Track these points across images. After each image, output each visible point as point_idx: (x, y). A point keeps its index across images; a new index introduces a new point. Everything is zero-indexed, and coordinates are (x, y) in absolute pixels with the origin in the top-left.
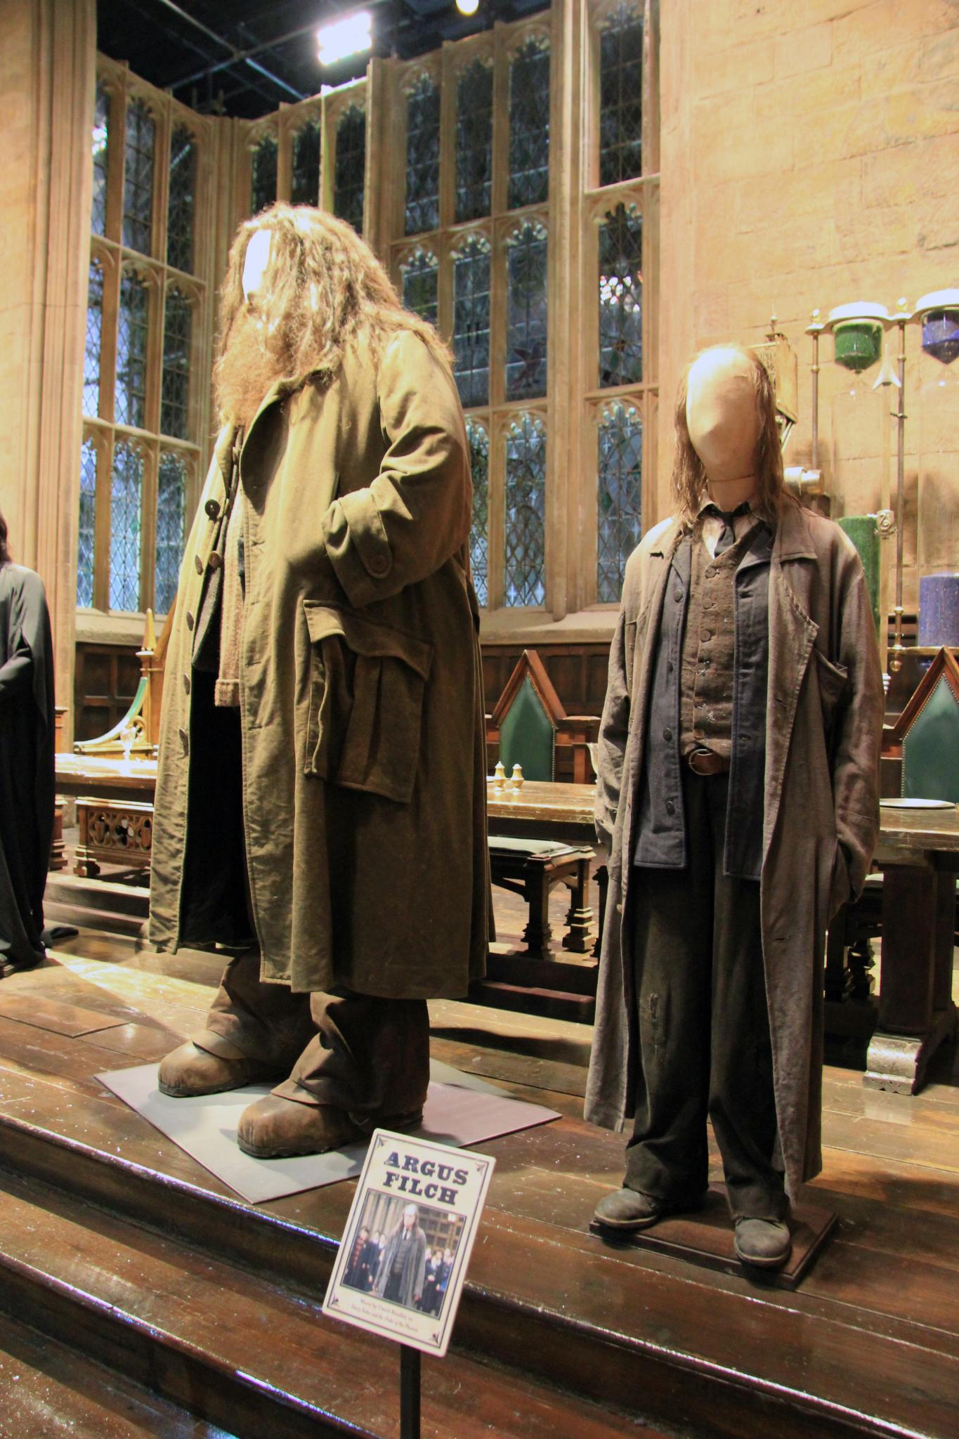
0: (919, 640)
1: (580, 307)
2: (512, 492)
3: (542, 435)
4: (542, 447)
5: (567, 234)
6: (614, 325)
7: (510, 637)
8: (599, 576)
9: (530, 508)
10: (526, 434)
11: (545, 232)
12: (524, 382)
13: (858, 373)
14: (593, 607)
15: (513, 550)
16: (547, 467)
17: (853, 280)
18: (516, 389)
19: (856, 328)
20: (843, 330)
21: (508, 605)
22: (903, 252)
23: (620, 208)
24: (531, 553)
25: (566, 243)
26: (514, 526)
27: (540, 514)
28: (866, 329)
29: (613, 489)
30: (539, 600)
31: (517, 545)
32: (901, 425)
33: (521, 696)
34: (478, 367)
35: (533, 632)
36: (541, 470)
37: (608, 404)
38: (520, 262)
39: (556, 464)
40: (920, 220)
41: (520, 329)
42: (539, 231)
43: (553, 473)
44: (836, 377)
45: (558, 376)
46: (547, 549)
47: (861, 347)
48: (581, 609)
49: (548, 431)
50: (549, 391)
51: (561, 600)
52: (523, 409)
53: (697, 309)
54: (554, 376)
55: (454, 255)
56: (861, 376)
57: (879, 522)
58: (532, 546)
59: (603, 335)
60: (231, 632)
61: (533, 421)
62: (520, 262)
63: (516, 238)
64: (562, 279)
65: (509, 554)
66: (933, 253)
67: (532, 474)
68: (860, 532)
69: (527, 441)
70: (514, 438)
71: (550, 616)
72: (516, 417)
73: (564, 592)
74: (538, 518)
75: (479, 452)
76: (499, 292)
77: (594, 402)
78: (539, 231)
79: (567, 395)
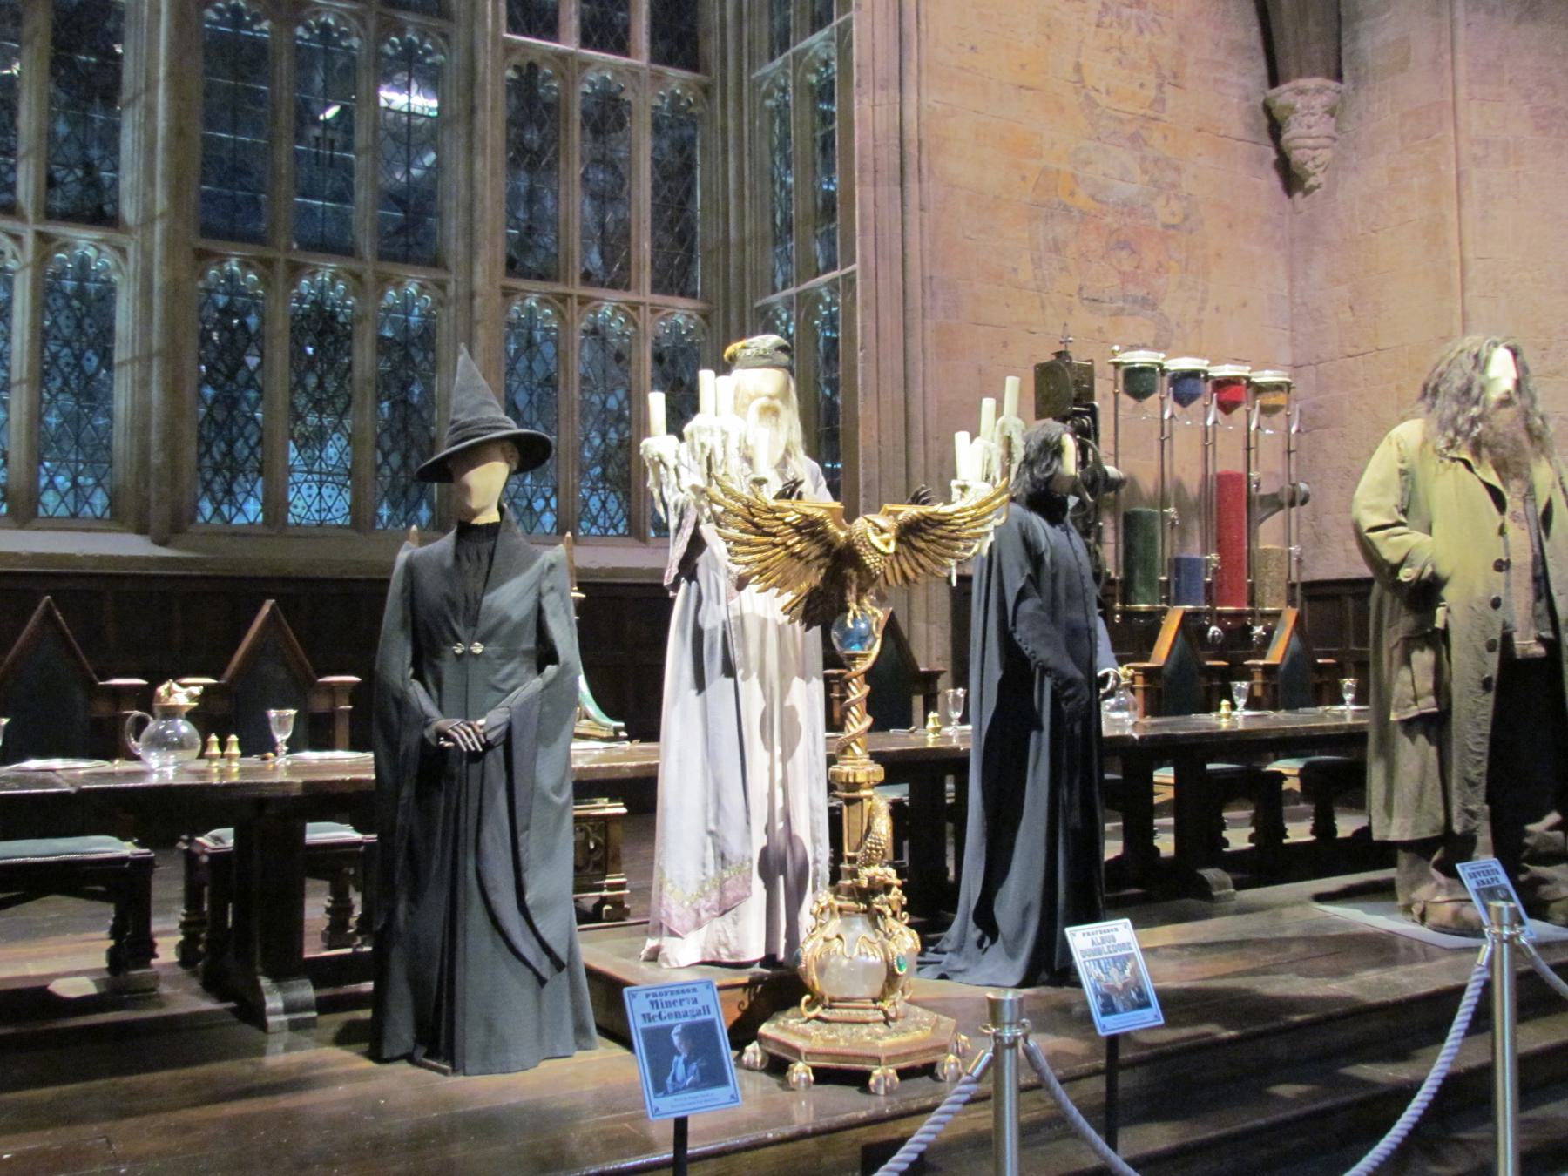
6: (522, 206)
12: (402, 239)
15: (386, 455)
23: (533, 67)
37: (524, 298)
55: (300, 31)
59: (511, 213)
65: (380, 460)
70: (388, 310)
77: (508, 293)
78: (428, 53)
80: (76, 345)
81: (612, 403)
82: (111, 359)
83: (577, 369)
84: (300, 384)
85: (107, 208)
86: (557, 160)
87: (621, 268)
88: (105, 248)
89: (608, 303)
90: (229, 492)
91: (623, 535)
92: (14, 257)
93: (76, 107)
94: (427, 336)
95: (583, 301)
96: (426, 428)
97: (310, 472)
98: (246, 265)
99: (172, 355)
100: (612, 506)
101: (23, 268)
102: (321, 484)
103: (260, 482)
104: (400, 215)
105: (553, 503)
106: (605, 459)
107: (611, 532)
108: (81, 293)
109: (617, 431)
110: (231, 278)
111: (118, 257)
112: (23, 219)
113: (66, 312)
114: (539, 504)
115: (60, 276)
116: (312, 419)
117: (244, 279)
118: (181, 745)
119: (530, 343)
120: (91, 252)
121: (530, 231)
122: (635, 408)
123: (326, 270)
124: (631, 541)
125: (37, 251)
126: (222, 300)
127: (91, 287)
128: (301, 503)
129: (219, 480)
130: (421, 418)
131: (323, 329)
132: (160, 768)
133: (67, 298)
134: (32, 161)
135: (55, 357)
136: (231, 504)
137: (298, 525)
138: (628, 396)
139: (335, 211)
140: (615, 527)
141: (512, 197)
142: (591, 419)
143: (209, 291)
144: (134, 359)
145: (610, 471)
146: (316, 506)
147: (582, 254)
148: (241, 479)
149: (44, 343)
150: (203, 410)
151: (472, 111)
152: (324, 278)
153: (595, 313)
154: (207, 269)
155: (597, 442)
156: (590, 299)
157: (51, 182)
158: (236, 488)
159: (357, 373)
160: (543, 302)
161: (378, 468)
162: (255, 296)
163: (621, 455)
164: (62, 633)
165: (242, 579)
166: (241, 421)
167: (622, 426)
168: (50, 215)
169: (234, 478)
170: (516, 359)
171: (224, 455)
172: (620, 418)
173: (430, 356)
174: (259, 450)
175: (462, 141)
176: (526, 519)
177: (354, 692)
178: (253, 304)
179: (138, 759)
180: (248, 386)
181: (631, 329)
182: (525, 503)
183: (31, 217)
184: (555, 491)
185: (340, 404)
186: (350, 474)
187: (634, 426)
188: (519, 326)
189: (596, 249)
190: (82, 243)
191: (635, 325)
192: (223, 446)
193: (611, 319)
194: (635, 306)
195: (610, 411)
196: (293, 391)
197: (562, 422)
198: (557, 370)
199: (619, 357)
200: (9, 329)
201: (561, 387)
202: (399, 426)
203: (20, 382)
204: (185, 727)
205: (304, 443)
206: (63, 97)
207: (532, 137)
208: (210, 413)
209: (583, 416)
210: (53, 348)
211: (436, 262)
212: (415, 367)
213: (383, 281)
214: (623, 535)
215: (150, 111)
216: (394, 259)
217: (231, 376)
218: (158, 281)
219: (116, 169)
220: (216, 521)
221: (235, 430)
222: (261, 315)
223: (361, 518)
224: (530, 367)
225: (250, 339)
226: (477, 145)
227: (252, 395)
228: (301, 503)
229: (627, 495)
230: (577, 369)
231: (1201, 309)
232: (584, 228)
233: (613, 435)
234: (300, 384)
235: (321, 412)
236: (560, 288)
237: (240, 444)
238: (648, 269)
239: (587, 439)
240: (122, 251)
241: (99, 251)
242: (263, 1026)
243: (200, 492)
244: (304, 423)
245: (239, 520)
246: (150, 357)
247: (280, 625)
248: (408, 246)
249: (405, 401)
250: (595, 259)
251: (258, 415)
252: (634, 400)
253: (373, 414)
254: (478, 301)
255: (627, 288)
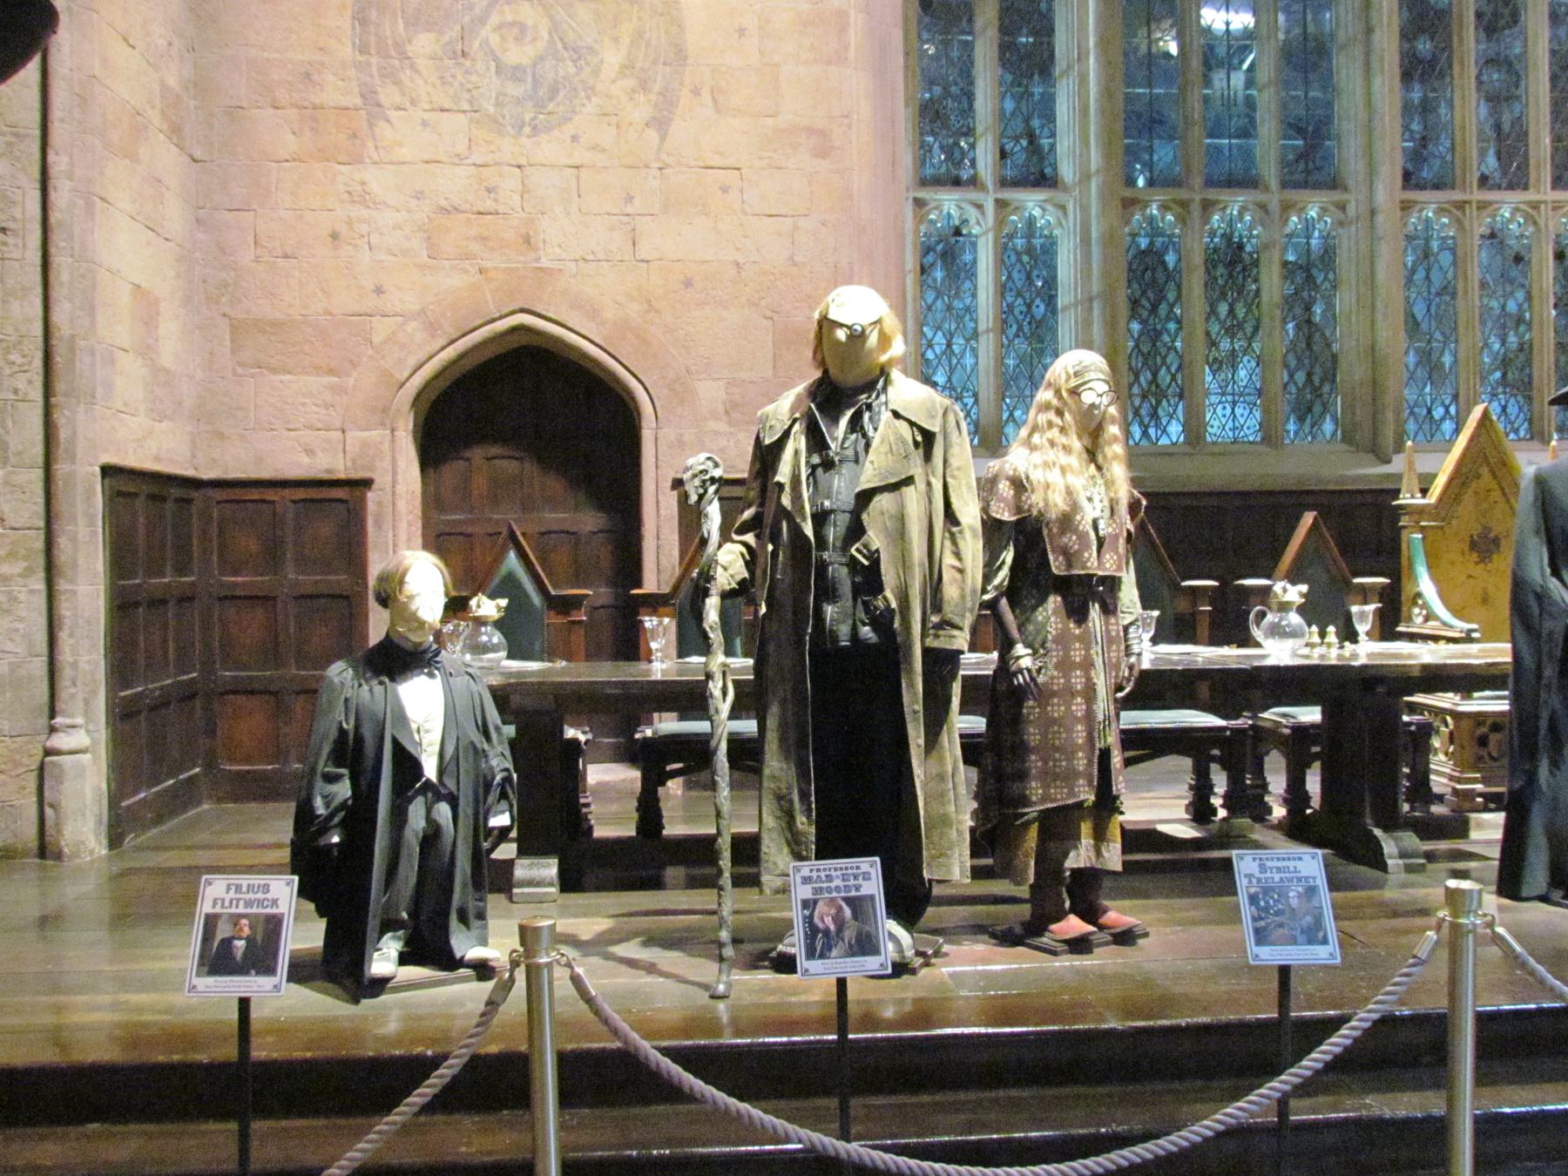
2: (1288, 303)
7: (1336, 483)
12: (1302, 166)
18: (1291, 173)
21: (1287, 441)
29: (1419, 311)
34: (1238, 137)
37: (1421, 210)
59: (1406, 128)
60: (402, 464)
65: (1286, 378)
70: (1290, 236)
75: (1241, 247)
77: (1406, 207)
80: (1027, 295)
81: (1512, 306)
82: (1055, 305)
83: (1475, 274)
84: (1213, 312)
85: (1048, 171)
86: (1450, 67)
87: (1518, 168)
88: (1049, 207)
89: (1507, 207)
90: (1154, 415)
91: (1524, 439)
92: (978, 223)
93: (1020, 85)
94: (1328, 255)
95: (1482, 206)
96: (1328, 346)
97: (1223, 394)
98: (1164, 207)
99: (1108, 296)
100: (1512, 410)
101: (985, 233)
102: (1234, 403)
103: (1180, 406)
104: (1301, 142)
105: (1452, 410)
106: (1505, 363)
107: (1512, 436)
108: (1030, 250)
109: (1517, 334)
110: (1151, 220)
111: (1060, 214)
112: (983, 188)
113: (1018, 266)
114: (1438, 413)
115: (1011, 237)
116: (1225, 345)
117: (1163, 220)
118: (1294, 634)
119: (1427, 254)
120: (1037, 212)
121: (1424, 141)
122: (1536, 309)
123: (1235, 202)
124: (1535, 444)
125: (996, 218)
126: (1143, 243)
127: (1037, 242)
128: (1216, 423)
129: (1146, 405)
130: (1323, 334)
131: (1232, 264)
132: (1277, 652)
133: (1018, 254)
134: (990, 138)
135: (1011, 306)
136: (1157, 426)
137: (1214, 443)
138: (1529, 297)
139: (1240, 147)
140: (1516, 431)
141: (1407, 109)
142: (1489, 324)
143: (1134, 235)
144: (1075, 305)
145: (1510, 375)
146: (1230, 424)
147: (1480, 159)
148: (1164, 403)
149: (1003, 296)
150: (1131, 344)
151: (1369, 31)
152: (1235, 212)
153: (1493, 216)
154: (1132, 215)
155: (1497, 346)
156: (1490, 203)
157: (1003, 154)
158: (1161, 412)
159: (1265, 297)
160: (1440, 211)
161: (1285, 386)
162: (1173, 235)
163: (1522, 357)
164: (1153, 543)
165: (1270, 493)
166: (1163, 351)
167: (1522, 328)
168: (1004, 183)
169: (1159, 403)
170: (1413, 271)
171: (1150, 383)
172: (1520, 320)
173: (1331, 276)
174: (1179, 377)
175: (1359, 64)
176: (1426, 427)
177: (1214, 596)
178: (1171, 242)
179: (1258, 645)
180: (1168, 319)
181: (1531, 229)
182: (1425, 411)
183: (991, 187)
184: (1455, 397)
185: (1249, 330)
186: (1260, 393)
187: (1535, 326)
188: (1417, 238)
189: (1492, 152)
190: (1030, 204)
191: (1535, 223)
192: (1149, 375)
193: (1510, 221)
194: (1535, 206)
195: (1510, 315)
196: (1207, 319)
197: (1461, 329)
198: (1455, 277)
199: (1518, 259)
200: (976, 287)
201: (1460, 294)
202: (1304, 345)
203: (988, 331)
204: (1294, 619)
205: (1216, 365)
206: (1009, 78)
207: (1424, 46)
208: (1137, 346)
209: (1483, 322)
210: (1010, 299)
211: (1334, 184)
212: (1316, 288)
213: (1287, 208)
214: (1524, 439)
215: (1083, 80)
216: (1297, 185)
217: (1154, 309)
218: (1094, 234)
219: (1053, 135)
220: (1144, 443)
221: (1159, 360)
222: (1178, 251)
223: (1270, 436)
224: (1428, 278)
225: (1169, 276)
226: (1375, 65)
227: (1172, 326)
228: (1216, 423)
229: (1529, 399)
230: (1475, 274)
232: (1480, 132)
233: (1512, 339)
234: (1213, 312)
235: (1232, 337)
236: (1457, 196)
237: (1163, 370)
238: (1549, 167)
239: (1486, 345)
240: (1063, 208)
241: (1044, 210)
242: (1383, 867)
243: (1130, 417)
244: (1217, 349)
245: (1164, 441)
246: (1091, 300)
247: (1321, 535)
249: (1309, 321)
250: (1492, 161)
251: (1178, 344)
252: (1535, 302)
253: (1281, 335)
254: (1380, 218)
255: (1526, 188)
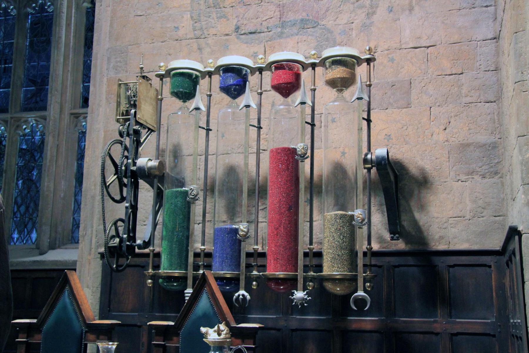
0: (214, 268)
1: (71, 56)
2: (21, 170)
3: (43, 135)
4: (43, 142)
5: (65, 10)
8: (73, 226)
9: (31, 180)
10: (33, 132)
11: (52, 7)
12: (34, 99)
13: (184, 102)
14: (69, 246)
16: (44, 156)
17: (199, 49)
19: (182, 74)
20: (175, 75)
21: (12, 244)
22: (227, 35)
24: (31, 211)
25: (64, 16)
26: (21, 191)
27: (38, 185)
28: (189, 76)
30: (34, 240)
31: (21, 205)
32: (207, 135)
33: (59, 305)
35: (24, 262)
36: (41, 156)
38: (36, 24)
39: (49, 153)
40: (236, 17)
41: (34, 67)
42: (49, 7)
43: (46, 159)
44: (171, 104)
45: (53, 98)
46: (40, 208)
47: (186, 86)
48: (59, 247)
49: (46, 132)
50: (48, 107)
51: (45, 241)
52: (32, 117)
53: (109, 59)
54: (51, 97)
56: (186, 104)
57: (190, 192)
58: (32, 205)
61: (37, 125)
62: (36, 24)
63: (34, 8)
64: (60, 38)
65: (16, 210)
66: (243, 36)
67: (35, 159)
68: (179, 199)
69: (33, 138)
70: (25, 135)
71: (37, 251)
72: (26, 122)
73: (48, 235)
74: (37, 187)
76: (21, 41)
77: (76, 116)
78: (49, 7)
79: (58, 111)
231: (369, 15)
248: (37, 102)
